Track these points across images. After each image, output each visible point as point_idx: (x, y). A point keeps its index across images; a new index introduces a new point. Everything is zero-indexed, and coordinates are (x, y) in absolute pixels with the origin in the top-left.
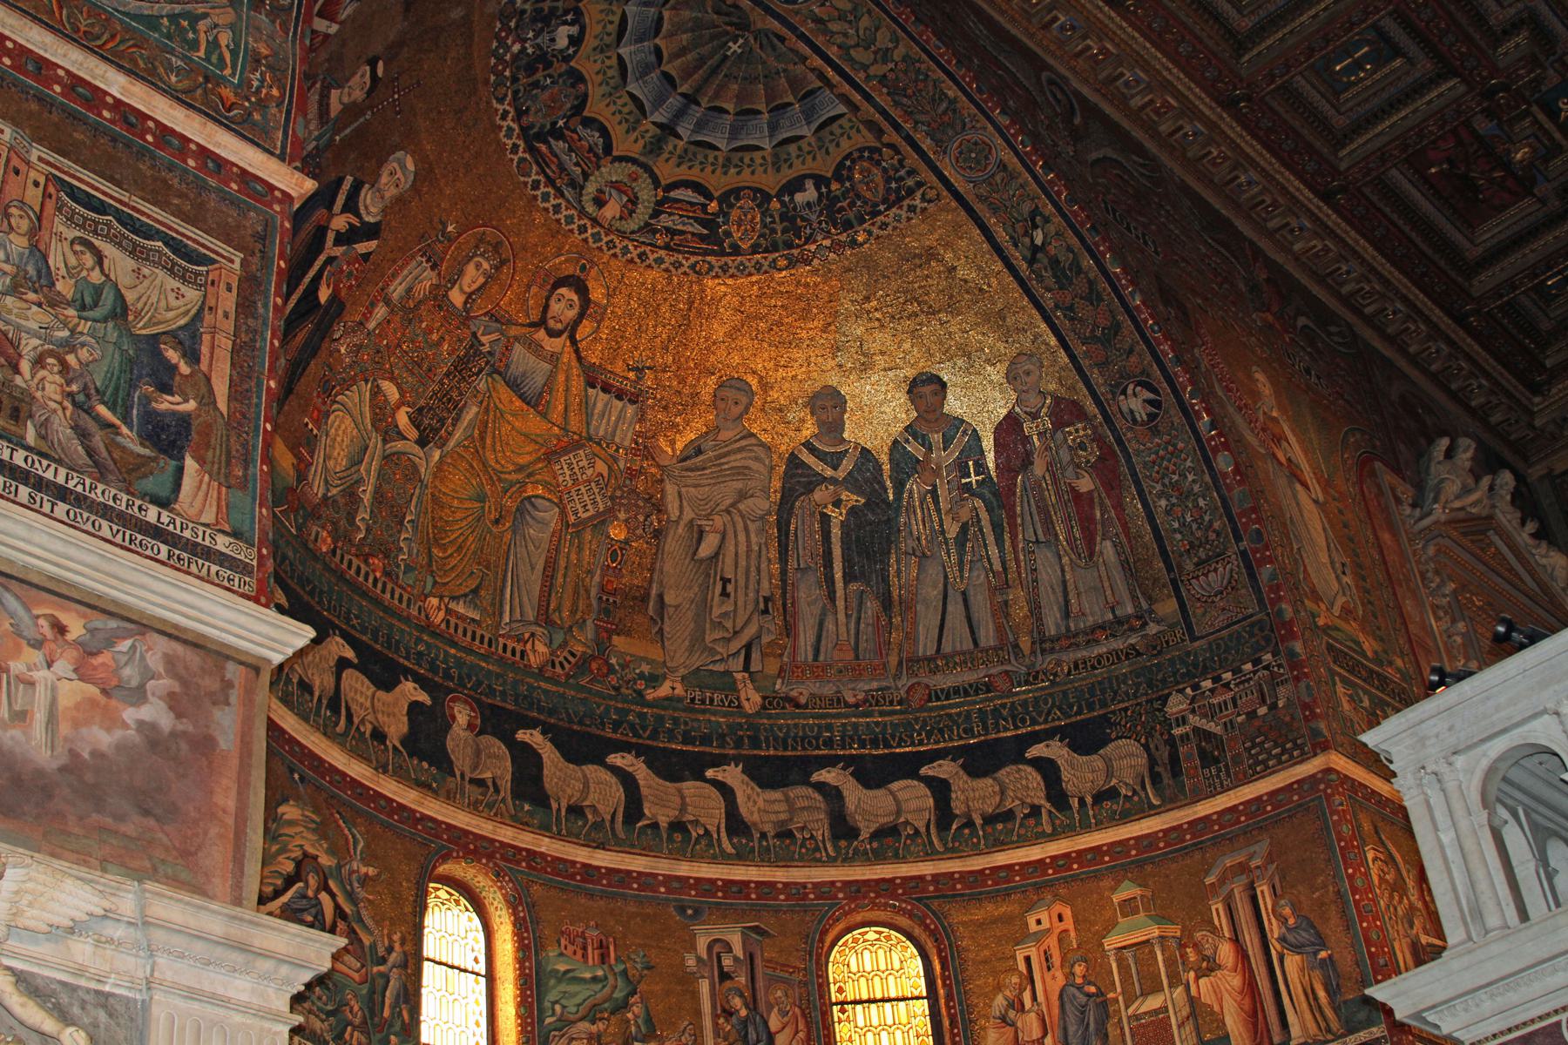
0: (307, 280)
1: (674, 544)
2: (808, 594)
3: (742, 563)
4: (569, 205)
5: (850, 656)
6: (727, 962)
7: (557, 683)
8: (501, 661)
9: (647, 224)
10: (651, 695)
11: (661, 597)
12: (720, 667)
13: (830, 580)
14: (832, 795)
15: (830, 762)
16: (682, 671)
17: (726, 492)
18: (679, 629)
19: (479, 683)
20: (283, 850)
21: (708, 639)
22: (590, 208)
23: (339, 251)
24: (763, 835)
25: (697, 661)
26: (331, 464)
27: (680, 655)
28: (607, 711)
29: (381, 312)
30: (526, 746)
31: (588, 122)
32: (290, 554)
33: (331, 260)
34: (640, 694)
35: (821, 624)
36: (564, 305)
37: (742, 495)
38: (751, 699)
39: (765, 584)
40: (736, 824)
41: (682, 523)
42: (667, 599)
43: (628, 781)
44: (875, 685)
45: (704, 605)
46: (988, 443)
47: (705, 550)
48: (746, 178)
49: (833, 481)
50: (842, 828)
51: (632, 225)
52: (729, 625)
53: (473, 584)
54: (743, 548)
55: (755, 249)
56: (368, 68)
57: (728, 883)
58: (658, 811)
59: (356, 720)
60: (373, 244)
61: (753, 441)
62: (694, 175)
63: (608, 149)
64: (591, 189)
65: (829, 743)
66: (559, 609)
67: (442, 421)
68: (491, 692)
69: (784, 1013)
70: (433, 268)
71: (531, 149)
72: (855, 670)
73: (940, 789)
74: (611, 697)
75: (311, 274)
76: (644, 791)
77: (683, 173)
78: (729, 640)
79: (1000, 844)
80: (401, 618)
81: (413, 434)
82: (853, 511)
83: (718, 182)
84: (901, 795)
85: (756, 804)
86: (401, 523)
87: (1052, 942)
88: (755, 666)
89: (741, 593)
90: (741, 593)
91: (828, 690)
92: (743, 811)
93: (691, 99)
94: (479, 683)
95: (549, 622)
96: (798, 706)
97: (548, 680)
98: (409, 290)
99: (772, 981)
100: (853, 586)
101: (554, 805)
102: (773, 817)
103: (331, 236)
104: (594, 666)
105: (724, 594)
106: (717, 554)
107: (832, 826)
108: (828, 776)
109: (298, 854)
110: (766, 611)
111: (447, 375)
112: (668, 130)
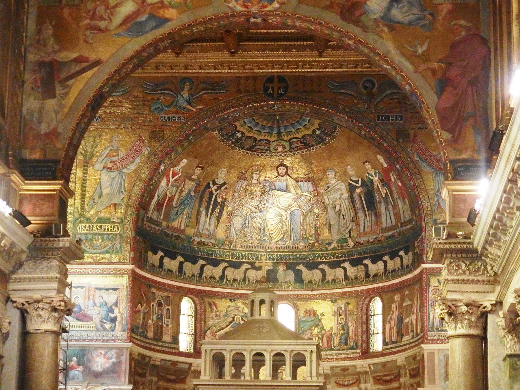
0: (212, 202)
1: (330, 209)
2: (361, 214)
3: (346, 211)
4: (269, 154)
5: (370, 229)
6: (341, 312)
7: (306, 252)
8: (292, 252)
9: (290, 148)
10: (329, 248)
11: (330, 223)
12: (344, 237)
13: (365, 210)
14: (366, 266)
15: (366, 258)
16: (336, 241)
17: (337, 195)
18: (335, 229)
19: (286, 258)
20: (229, 317)
21: (341, 231)
22: (275, 151)
23: (218, 192)
24: (352, 279)
25: (339, 237)
26: (236, 229)
27: (336, 237)
28: (319, 254)
29: (236, 194)
30: (298, 270)
31: (260, 140)
32: (228, 253)
33: (217, 194)
34: (327, 248)
35: (364, 222)
36: (282, 170)
37: (342, 195)
38: (351, 244)
39: (352, 214)
40: (346, 277)
41: (330, 205)
42: (331, 223)
43: (323, 271)
44: (375, 237)
45: (339, 223)
46: (382, 175)
47: (337, 209)
48: (303, 134)
49: (359, 187)
50: (367, 275)
51: (287, 149)
52: (345, 226)
53: (282, 236)
54: (345, 207)
55: (317, 144)
56: (198, 168)
57: (343, 292)
58: (329, 278)
59: (251, 281)
60: (226, 186)
61: (339, 181)
62: (292, 136)
63: (269, 141)
64: (272, 149)
65: (367, 253)
66: (306, 234)
67: (264, 204)
68: (290, 259)
69: (352, 322)
70: (245, 180)
71: (252, 151)
72: (372, 232)
73: (385, 263)
74: (321, 251)
75: (214, 198)
76: (327, 273)
77: (289, 138)
78: (345, 230)
79: (393, 278)
80: (263, 252)
81: (258, 211)
82: (365, 194)
83: (300, 135)
84: (379, 265)
85: (352, 271)
86: (261, 231)
87: (397, 303)
88: (352, 236)
89: (347, 218)
90: (347, 218)
91: (366, 239)
92: (348, 274)
93: (279, 127)
94: (286, 258)
95: (303, 238)
96: (361, 244)
97: (304, 252)
98: (241, 186)
99: (350, 314)
100: (369, 211)
101: (305, 282)
102: (354, 274)
103: (214, 192)
104: (316, 245)
105: (344, 219)
106: (340, 210)
107: (366, 274)
108: (366, 262)
109: (233, 316)
110: (353, 221)
111: (261, 195)
112: (279, 133)
